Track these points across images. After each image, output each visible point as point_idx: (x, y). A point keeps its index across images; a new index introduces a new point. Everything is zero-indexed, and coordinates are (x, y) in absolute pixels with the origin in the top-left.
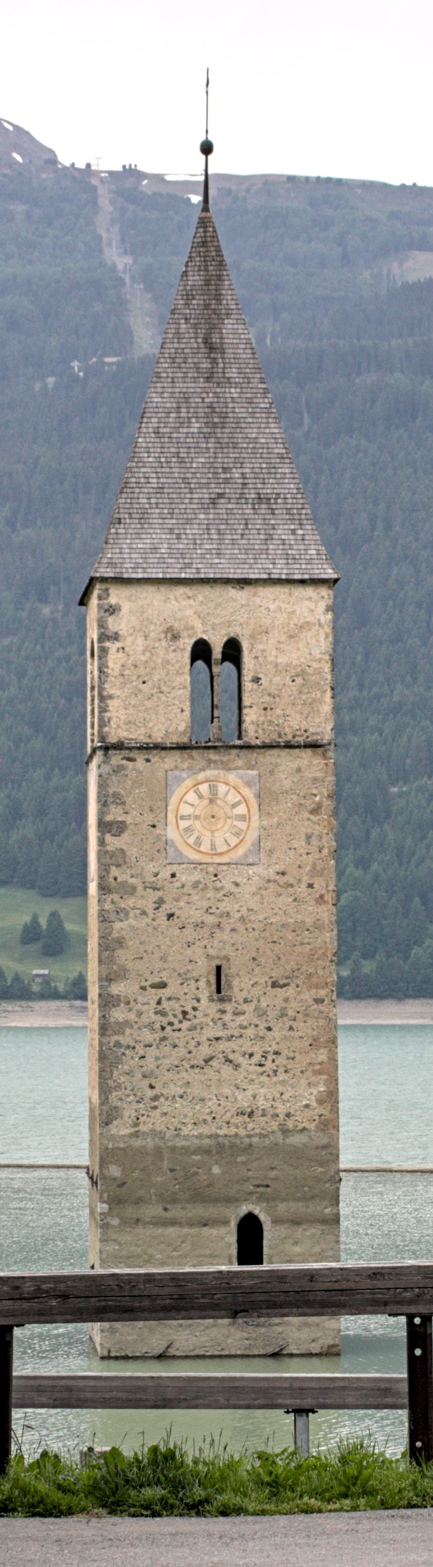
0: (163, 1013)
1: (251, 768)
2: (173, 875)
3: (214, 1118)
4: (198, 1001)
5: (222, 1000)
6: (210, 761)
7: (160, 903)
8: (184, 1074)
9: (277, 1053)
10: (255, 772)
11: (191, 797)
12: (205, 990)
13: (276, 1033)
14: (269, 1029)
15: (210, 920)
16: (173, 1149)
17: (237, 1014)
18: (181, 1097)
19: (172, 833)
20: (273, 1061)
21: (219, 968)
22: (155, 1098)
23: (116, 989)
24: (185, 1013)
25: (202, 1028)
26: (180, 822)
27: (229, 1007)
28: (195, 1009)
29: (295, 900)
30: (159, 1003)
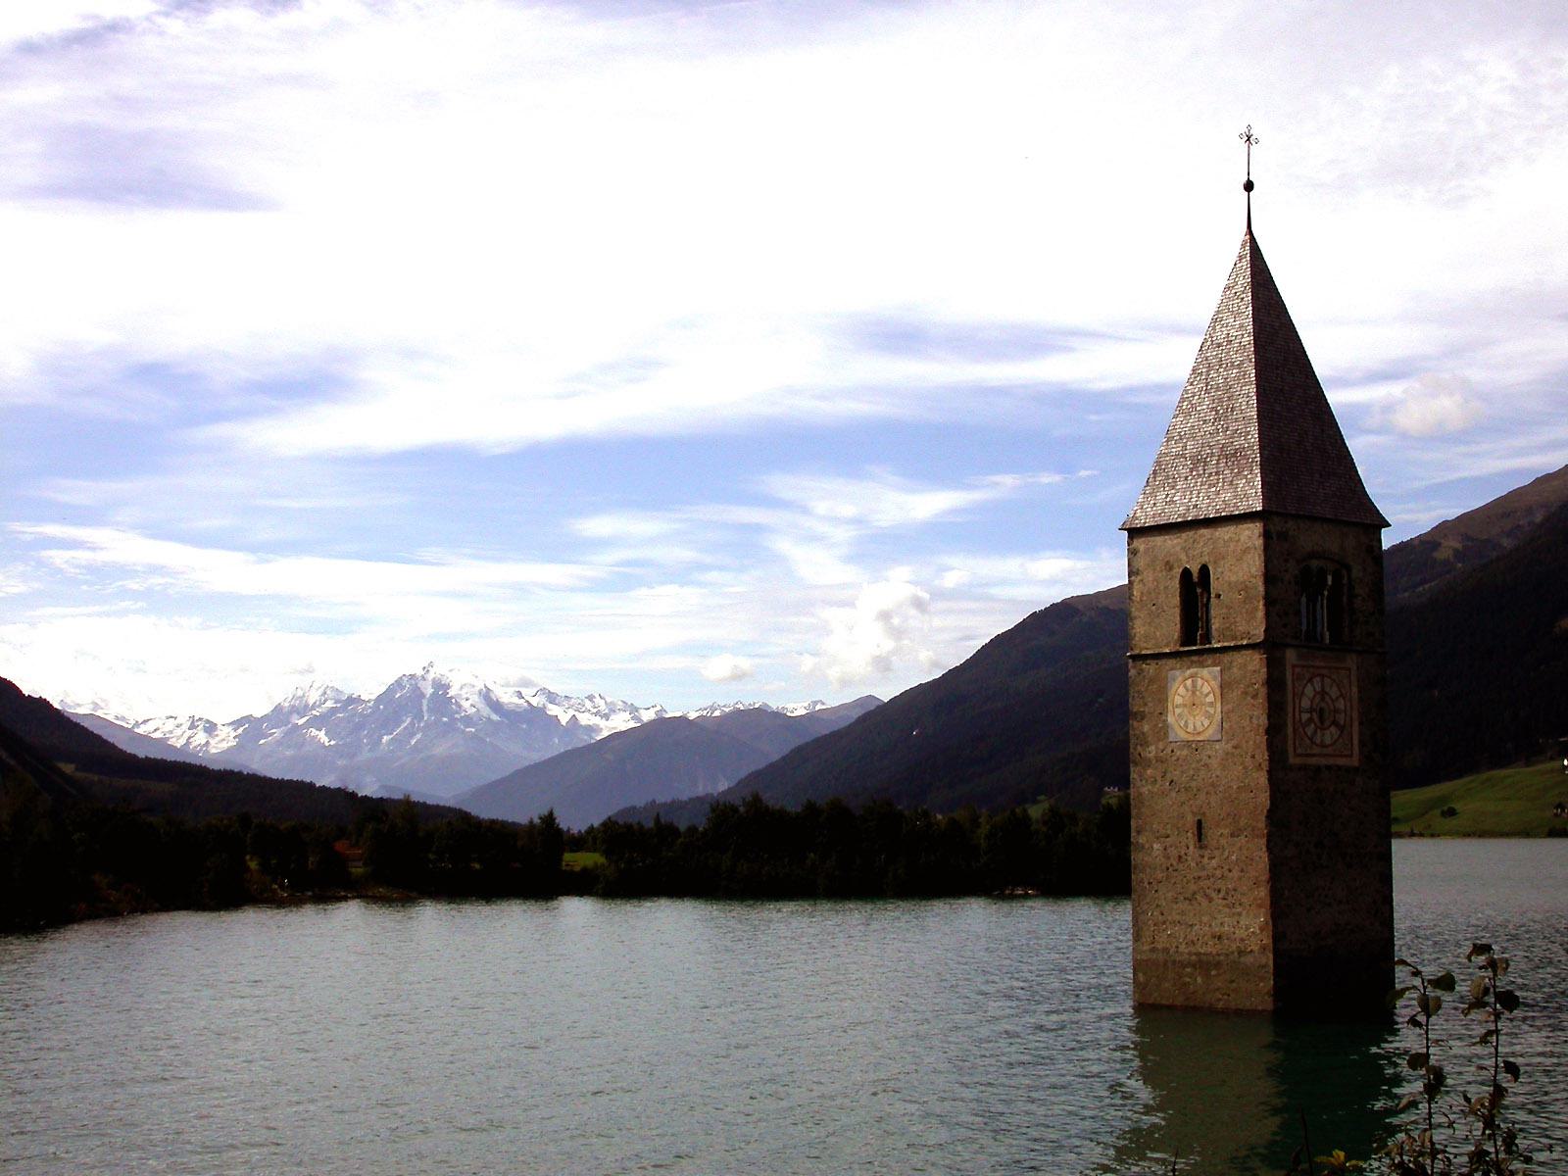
2: (1172, 751)
4: (1188, 848)
5: (1201, 847)
6: (1192, 662)
8: (1180, 905)
10: (1219, 668)
12: (1190, 838)
13: (1236, 873)
15: (1194, 784)
16: (1174, 962)
19: (1171, 719)
21: (1199, 822)
24: (1180, 857)
26: (1176, 710)
27: (1207, 853)
28: (1186, 854)
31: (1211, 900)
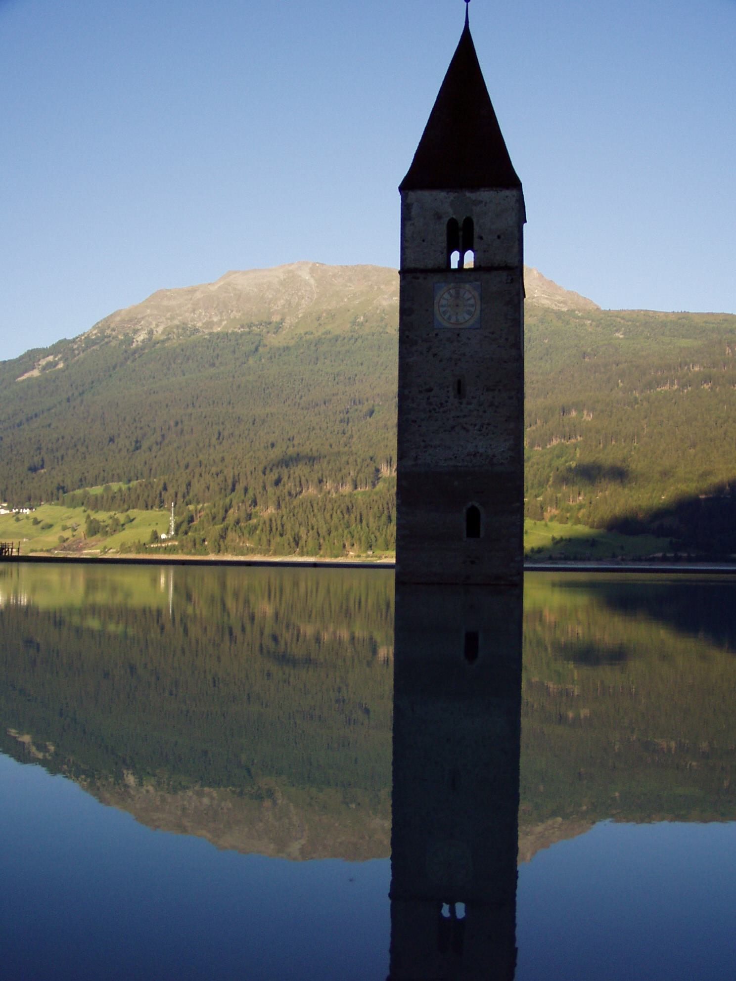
0: (431, 404)
1: (477, 280)
3: (456, 457)
4: (449, 397)
7: (429, 349)
9: (488, 424)
10: (478, 283)
11: (446, 296)
14: (485, 412)
17: (469, 404)
18: (439, 446)
20: (487, 428)
21: (459, 382)
22: (426, 447)
23: (406, 392)
24: (441, 404)
25: (450, 411)
29: (499, 346)
30: (428, 399)
31: (468, 431)
